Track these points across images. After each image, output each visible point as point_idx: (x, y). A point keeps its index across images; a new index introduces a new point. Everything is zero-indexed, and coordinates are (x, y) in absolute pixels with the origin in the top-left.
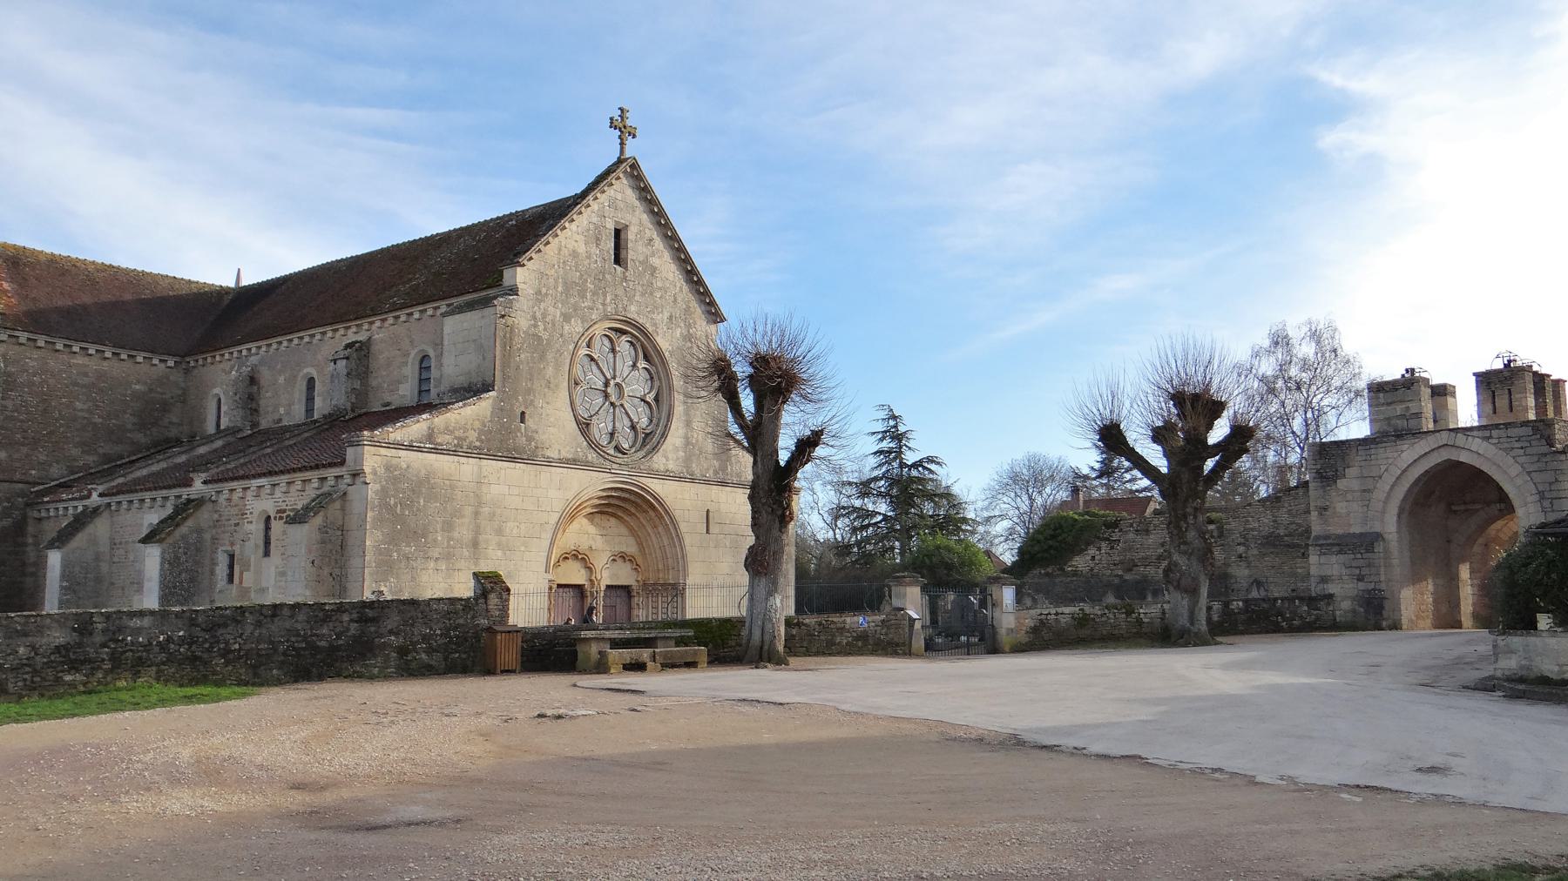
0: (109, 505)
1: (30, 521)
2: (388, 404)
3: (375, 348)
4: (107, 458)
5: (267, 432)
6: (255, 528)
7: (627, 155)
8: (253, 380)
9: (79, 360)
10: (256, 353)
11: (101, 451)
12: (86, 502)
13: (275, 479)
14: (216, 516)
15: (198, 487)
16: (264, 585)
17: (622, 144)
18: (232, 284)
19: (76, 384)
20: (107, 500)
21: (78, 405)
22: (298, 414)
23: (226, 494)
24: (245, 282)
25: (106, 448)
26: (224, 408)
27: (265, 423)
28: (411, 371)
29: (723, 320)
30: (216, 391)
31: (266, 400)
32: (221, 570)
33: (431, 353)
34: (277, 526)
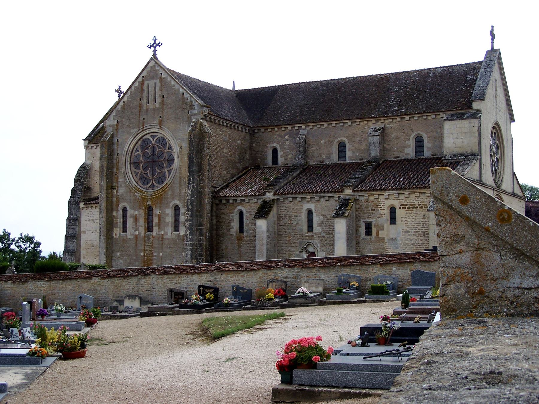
0: (278, 199)
1: (214, 205)
2: (398, 157)
3: (386, 131)
4: (233, 176)
5: (316, 167)
6: (387, 212)
7: (495, 48)
8: (305, 141)
9: (225, 129)
10: (305, 130)
11: (230, 172)
12: (263, 198)
13: (402, 191)
14: (358, 206)
15: (348, 192)
16: (392, 236)
17: (493, 43)
18: (231, 88)
19: (224, 140)
20: (276, 197)
21: (225, 151)
22: (335, 159)
23: (366, 197)
24: (237, 89)
25: (233, 171)
26: (280, 153)
27: (312, 163)
28: (411, 143)
29: (514, 121)
30: (275, 145)
31: (313, 150)
32: (363, 230)
33: (425, 136)
34: (400, 213)
